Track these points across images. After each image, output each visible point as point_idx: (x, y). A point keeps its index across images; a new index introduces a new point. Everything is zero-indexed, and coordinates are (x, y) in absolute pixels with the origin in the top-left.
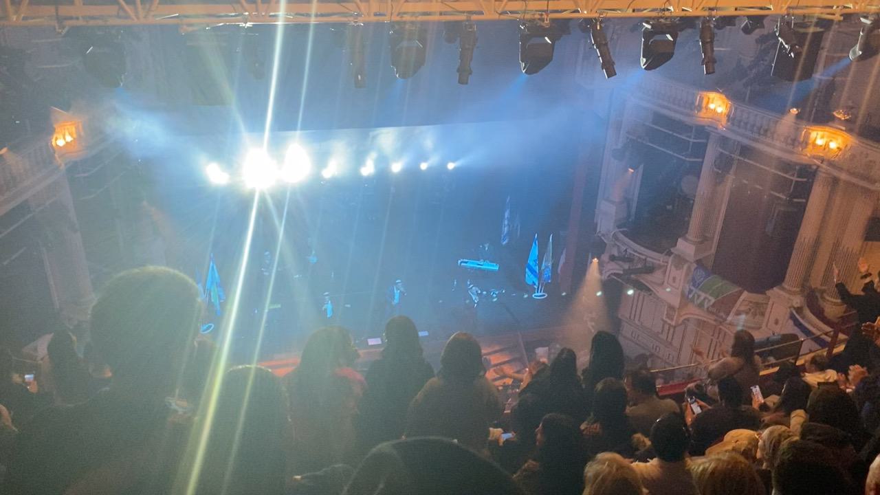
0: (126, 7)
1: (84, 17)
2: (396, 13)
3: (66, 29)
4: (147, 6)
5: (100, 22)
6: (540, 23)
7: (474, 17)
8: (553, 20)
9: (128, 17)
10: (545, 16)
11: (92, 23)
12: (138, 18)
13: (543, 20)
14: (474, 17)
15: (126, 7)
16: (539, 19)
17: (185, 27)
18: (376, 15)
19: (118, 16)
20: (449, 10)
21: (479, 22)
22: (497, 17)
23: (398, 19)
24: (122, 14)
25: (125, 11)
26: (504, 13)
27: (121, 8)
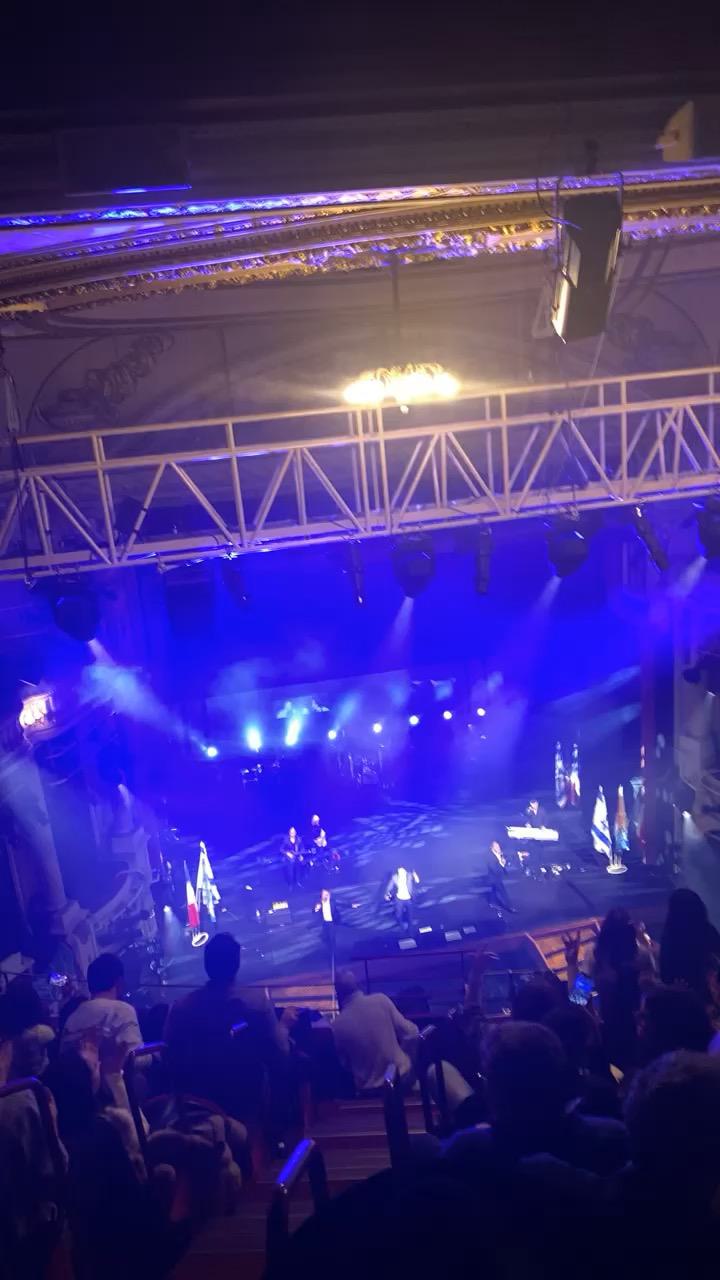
0: (99, 550)
1: (54, 567)
3: (35, 582)
4: (122, 547)
5: (72, 570)
6: (568, 516)
8: (581, 512)
9: (100, 560)
10: (572, 509)
11: (63, 571)
13: (569, 513)
15: (99, 550)
16: (567, 513)
17: (163, 565)
18: (374, 529)
19: (91, 562)
20: (456, 514)
21: (492, 525)
22: (514, 516)
23: (400, 531)
25: (98, 555)
26: (522, 510)
27: (94, 552)
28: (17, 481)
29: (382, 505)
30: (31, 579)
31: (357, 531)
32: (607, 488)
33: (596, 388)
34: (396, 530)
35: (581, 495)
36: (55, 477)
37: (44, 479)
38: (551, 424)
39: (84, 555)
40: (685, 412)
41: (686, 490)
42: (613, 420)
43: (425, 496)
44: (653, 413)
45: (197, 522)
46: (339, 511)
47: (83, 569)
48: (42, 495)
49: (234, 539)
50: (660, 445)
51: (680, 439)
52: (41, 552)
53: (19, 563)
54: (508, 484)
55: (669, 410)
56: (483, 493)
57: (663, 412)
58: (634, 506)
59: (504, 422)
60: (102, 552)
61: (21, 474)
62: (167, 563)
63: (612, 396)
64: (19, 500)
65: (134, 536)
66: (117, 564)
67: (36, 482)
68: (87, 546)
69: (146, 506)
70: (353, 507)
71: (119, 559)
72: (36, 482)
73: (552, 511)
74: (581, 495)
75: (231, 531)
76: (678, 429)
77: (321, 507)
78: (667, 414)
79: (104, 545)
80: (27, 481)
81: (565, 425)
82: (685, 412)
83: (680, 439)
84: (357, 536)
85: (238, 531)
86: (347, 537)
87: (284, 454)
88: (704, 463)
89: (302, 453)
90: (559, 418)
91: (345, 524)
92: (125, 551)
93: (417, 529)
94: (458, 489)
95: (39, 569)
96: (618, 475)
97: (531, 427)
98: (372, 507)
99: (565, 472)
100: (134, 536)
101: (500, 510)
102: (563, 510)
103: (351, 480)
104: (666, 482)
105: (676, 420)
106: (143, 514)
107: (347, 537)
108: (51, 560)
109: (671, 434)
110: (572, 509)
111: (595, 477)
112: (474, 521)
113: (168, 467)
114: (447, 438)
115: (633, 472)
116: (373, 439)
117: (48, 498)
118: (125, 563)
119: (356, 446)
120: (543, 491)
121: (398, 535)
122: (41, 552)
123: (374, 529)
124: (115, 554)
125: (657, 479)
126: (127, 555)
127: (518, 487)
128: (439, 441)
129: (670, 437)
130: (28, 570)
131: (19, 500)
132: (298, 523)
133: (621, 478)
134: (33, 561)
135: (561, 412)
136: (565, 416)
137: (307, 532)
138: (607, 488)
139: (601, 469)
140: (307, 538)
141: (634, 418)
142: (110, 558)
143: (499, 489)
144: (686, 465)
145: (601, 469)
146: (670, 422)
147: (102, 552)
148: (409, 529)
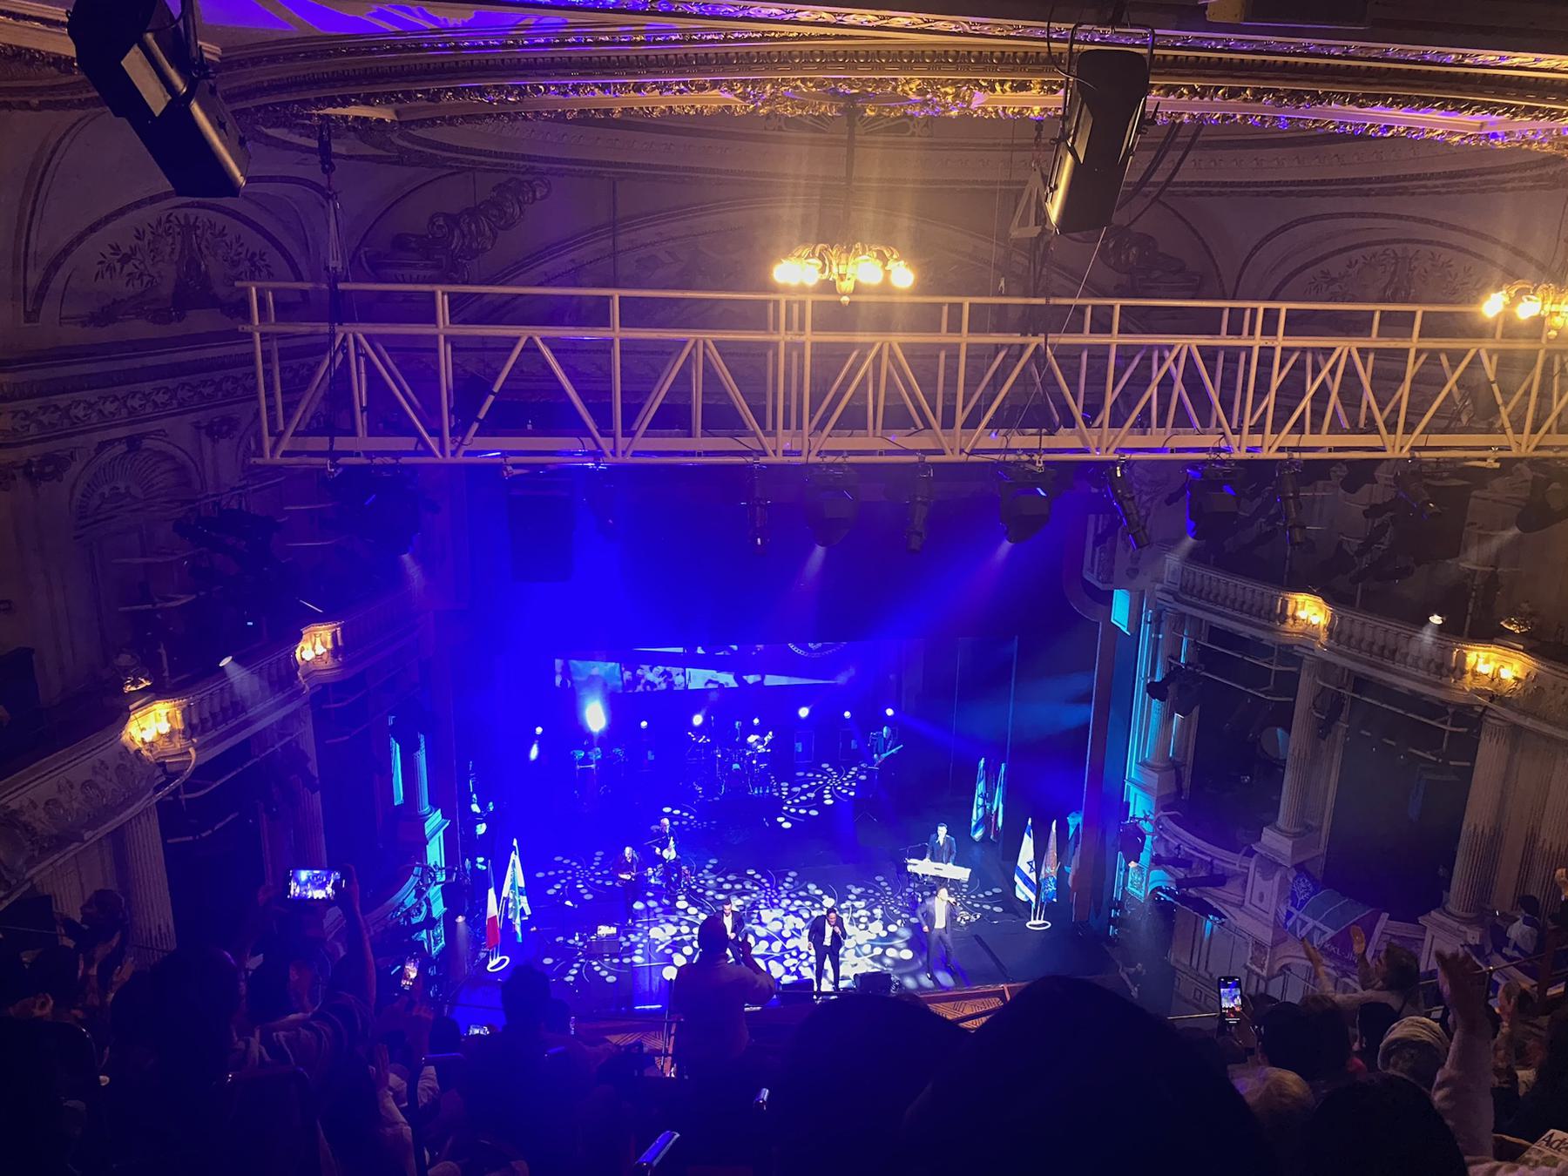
1: (368, 454)
2: (815, 452)
5: (389, 460)
7: (929, 459)
9: (429, 452)
10: (1036, 457)
11: (377, 461)
12: (442, 451)
13: (1034, 463)
14: (930, 459)
19: (416, 453)
21: (934, 464)
22: (963, 458)
23: (819, 459)
24: (420, 448)
26: (974, 452)
27: (422, 440)
28: (333, 335)
29: (800, 426)
30: (336, 466)
31: (765, 454)
32: (1083, 439)
33: (1080, 310)
34: (813, 459)
35: (1048, 442)
36: (381, 337)
37: (368, 337)
38: (1023, 347)
39: (407, 443)
40: (1190, 357)
41: (1179, 450)
42: (1098, 355)
43: (853, 420)
44: (1151, 347)
45: (559, 419)
46: (744, 427)
47: (404, 460)
48: (362, 359)
49: (607, 444)
50: (1153, 390)
51: (1179, 387)
52: (352, 432)
53: (321, 443)
54: (960, 417)
55: (1170, 348)
56: (928, 426)
57: (1161, 348)
58: (1114, 463)
59: (965, 339)
60: (432, 443)
61: (337, 329)
62: (515, 466)
63: (1102, 324)
64: (333, 360)
65: (475, 426)
66: (449, 459)
67: (356, 340)
68: (412, 431)
69: (496, 389)
70: (763, 427)
71: (454, 453)
72: (356, 340)
73: (1011, 457)
74: (1048, 442)
75: (602, 435)
76: (1178, 374)
77: (722, 418)
78: (1167, 354)
79: (436, 432)
80: (345, 339)
81: (1039, 354)
82: (1190, 357)
83: (1179, 387)
84: (762, 460)
85: (614, 436)
86: (750, 459)
87: (685, 342)
88: (1205, 423)
89: (705, 345)
90: (1034, 341)
91: (749, 443)
92: (461, 444)
93: (840, 459)
94: (897, 418)
95: (349, 454)
96: (1097, 423)
97: (998, 348)
98: (787, 426)
99: (1034, 411)
100: (475, 426)
101: (948, 450)
102: (1025, 458)
103: (764, 395)
104: (1155, 437)
105: (1176, 359)
106: (491, 398)
107: (750, 459)
108: (362, 443)
109: (1167, 382)
110: (1036, 457)
111: (1069, 422)
112: (915, 459)
113: (531, 348)
114: (892, 356)
115: (1117, 421)
116: (797, 339)
117: (369, 362)
118: (460, 458)
119: (776, 344)
120: (1003, 431)
121: (816, 465)
122: (352, 432)
123: (786, 453)
124: (449, 447)
125: (1144, 433)
126: (463, 449)
127: (971, 423)
128: (879, 356)
129: (1167, 382)
130: (333, 455)
131: (333, 360)
132: (690, 435)
133: (1100, 426)
134: (341, 443)
135: (1035, 335)
136: (1040, 339)
137: (700, 446)
138: (1083, 439)
139: (1078, 412)
140: (699, 455)
141: (1125, 354)
142: (442, 451)
143: (948, 423)
144: (1183, 421)
145: (1078, 412)
146: (1169, 363)
147: (432, 443)
148: (829, 459)
